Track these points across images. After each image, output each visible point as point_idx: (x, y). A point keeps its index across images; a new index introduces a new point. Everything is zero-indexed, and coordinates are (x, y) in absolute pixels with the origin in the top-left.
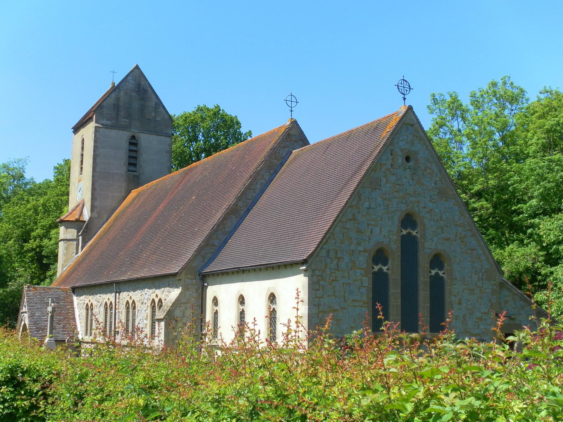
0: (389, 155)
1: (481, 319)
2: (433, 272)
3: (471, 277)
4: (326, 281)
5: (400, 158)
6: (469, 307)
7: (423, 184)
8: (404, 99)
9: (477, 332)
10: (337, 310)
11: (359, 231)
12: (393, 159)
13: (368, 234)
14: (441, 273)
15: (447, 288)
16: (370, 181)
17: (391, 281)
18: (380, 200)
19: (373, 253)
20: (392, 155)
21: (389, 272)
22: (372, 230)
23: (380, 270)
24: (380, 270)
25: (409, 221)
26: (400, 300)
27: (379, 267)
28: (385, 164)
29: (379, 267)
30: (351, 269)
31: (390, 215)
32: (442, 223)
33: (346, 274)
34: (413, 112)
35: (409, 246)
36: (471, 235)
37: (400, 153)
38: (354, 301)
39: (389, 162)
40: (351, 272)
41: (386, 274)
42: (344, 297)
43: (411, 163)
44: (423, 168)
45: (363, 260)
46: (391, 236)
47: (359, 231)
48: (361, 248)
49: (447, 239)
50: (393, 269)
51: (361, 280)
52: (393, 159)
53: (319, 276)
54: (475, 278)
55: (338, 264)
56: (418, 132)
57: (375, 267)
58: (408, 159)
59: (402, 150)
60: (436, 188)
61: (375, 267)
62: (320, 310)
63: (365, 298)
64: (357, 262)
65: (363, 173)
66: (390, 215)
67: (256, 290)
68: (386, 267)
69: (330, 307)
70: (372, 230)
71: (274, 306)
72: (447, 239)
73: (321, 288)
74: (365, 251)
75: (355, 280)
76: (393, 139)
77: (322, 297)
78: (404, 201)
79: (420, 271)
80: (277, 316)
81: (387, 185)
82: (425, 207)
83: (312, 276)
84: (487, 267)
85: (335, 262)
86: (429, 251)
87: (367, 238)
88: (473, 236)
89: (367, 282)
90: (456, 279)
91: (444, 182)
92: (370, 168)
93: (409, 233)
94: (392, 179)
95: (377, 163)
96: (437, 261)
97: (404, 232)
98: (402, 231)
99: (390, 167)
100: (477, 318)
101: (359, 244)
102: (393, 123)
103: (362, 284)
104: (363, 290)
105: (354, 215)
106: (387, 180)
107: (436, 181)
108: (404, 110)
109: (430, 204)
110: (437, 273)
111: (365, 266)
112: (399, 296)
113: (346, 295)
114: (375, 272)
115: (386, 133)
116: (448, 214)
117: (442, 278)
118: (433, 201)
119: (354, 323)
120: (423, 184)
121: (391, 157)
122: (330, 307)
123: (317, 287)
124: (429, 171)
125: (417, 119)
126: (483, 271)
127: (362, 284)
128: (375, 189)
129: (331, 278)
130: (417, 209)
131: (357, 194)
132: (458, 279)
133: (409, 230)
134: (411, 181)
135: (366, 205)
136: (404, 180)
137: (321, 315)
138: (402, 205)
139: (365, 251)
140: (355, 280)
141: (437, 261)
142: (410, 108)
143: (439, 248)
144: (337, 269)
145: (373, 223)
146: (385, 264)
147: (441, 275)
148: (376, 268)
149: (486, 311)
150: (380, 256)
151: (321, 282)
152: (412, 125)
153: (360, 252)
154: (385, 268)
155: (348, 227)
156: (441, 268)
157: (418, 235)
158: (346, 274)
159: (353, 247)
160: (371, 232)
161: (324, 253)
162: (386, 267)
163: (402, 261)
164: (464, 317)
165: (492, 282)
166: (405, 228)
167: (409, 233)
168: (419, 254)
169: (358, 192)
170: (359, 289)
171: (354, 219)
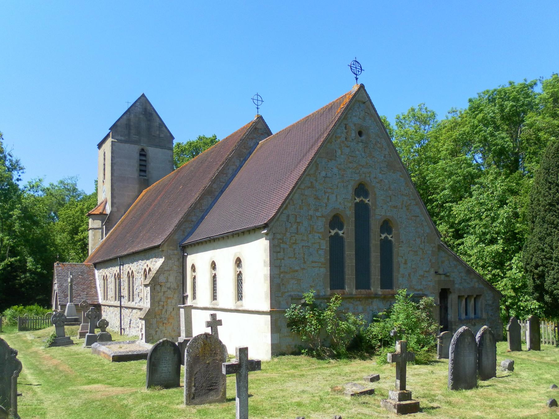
0: (344, 128)
1: (423, 276)
2: (383, 236)
3: (415, 240)
4: (286, 243)
5: (353, 132)
6: (413, 266)
7: (374, 157)
8: (357, 79)
9: (419, 287)
10: (297, 271)
11: (317, 198)
12: (347, 133)
13: (326, 201)
14: (389, 237)
15: (395, 250)
16: (326, 152)
17: (346, 244)
18: (335, 170)
19: (330, 218)
20: (346, 128)
21: (344, 236)
22: (328, 197)
23: (337, 234)
24: (337, 234)
25: (361, 190)
26: (354, 261)
27: (335, 231)
28: (340, 137)
29: (335, 231)
30: (310, 233)
31: (345, 184)
32: (390, 192)
33: (305, 238)
34: (365, 90)
35: (362, 213)
36: (415, 203)
37: (354, 128)
38: (313, 262)
39: (344, 136)
40: (310, 236)
41: (342, 238)
42: (304, 258)
43: (363, 138)
44: (374, 143)
45: (321, 225)
46: (346, 203)
47: (317, 198)
48: (318, 214)
49: (395, 207)
50: (348, 233)
51: (319, 243)
52: (347, 133)
53: (280, 239)
54: (418, 241)
55: (297, 228)
56: (369, 109)
57: (331, 231)
58: (360, 134)
59: (355, 125)
60: (385, 161)
61: (331, 231)
62: (282, 270)
63: (323, 260)
64: (315, 227)
65: (319, 144)
66: (345, 184)
67: (224, 256)
68: (342, 232)
69: (291, 268)
70: (328, 197)
71: (240, 270)
72: (395, 207)
73: (282, 251)
74: (322, 216)
75: (314, 243)
76: (346, 114)
77: (283, 259)
78: (357, 171)
79: (372, 235)
80: (243, 278)
81: (342, 156)
82: (375, 178)
83: (273, 239)
84: (427, 231)
85: (295, 227)
86: (379, 217)
87: (325, 205)
88: (416, 205)
89: (325, 245)
90: (402, 242)
91: (392, 156)
92: (326, 139)
93: (362, 201)
94: (347, 151)
95: (332, 136)
96: (386, 226)
97: (358, 200)
98: (355, 199)
99: (344, 140)
100: (420, 276)
101: (317, 210)
102: (347, 100)
103: (320, 246)
105: (312, 182)
106: (342, 152)
107: (385, 155)
108: (356, 88)
109: (380, 175)
110: (386, 237)
111: (323, 230)
112: (354, 257)
113: (306, 257)
114: (331, 236)
115: (339, 111)
116: (395, 185)
117: (390, 241)
118: (383, 172)
119: (313, 282)
120: (374, 157)
121: (345, 131)
122: (291, 268)
123: (278, 250)
124: (379, 145)
125: (369, 97)
126: (425, 235)
127: (320, 246)
128: (331, 160)
129: (292, 241)
130: (369, 179)
131: (314, 163)
132: (404, 242)
133: (362, 198)
134: (363, 154)
135: (323, 174)
136: (357, 152)
137: (282, 275)
138: (356, 175)
139: (322, 216)
140: (314, 243)
141: (386, 226)
142: (362, 86)
143: (388, 214)
144: (297, 233)
145: (329, 191)
146: (341, 229)
147: (390, 238)
148: (333, 233)
149: (428, 269)
150: (336, 221)
151: (282, 245)
152: (364, 103)
153: (318, 217)
154: (340, 233)
155: (306, 193)
156: (390, 232)
157: (370, 203)
158: (305, 238)
159: (311, 213)
160: (328, 199)
161: (284, 218)
162: (342, 232)
163: (356, 227)
164: (409, 275)
165: (433, 245)
166: (359, 197)
167: (362, 201)
168: (371, 220)
169: (316, 162)
170: (317, 251)
171: (312, 187)
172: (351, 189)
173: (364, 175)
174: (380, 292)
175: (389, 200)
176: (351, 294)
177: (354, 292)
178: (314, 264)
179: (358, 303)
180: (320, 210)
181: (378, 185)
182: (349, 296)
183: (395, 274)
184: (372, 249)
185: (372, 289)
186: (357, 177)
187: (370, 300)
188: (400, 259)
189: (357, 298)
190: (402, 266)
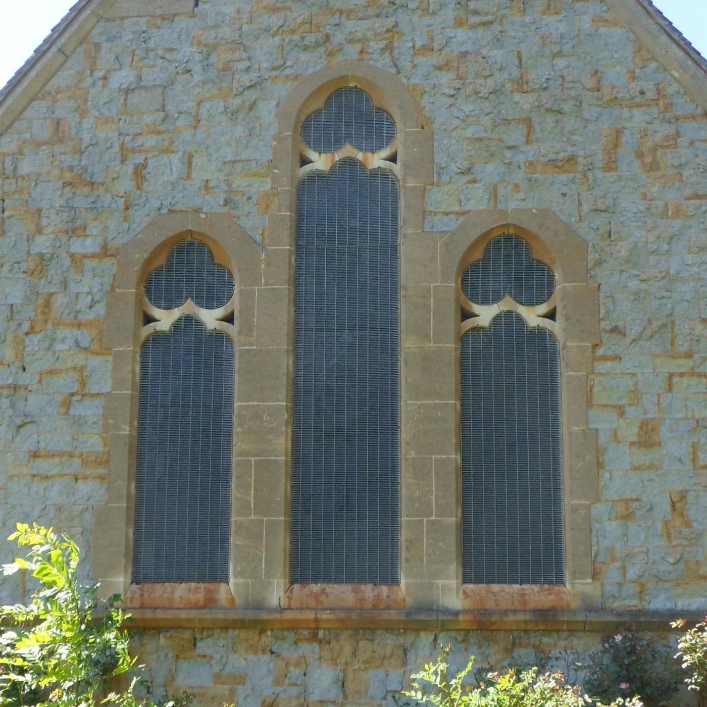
13: (126, 184)
27: (177, 313)
30: (32, 331)
38: (35, 455)
40: (33, 343)
46: (239, 183)
51: (80, 369)
57: (156, 312)
63: (93, 443)
68: (219, 312)
86: (452, 224)
89: (112, 376)
101: (75, 230)
103: (83, 383)
104: (90, 410)
127: (83, 383)
132: (632, 334)
138: (304, 57)
146: (210, 301)
153: (77, 261)
154: (210, 318)
157: (397, 168)
162: (219, 312)
166: (326, 145)
172: (271, 115)
173: (353, 51)
174: (453, 593)
175: (516, 135)
176: (259, 606)
177: (276, 593)
178: (43, 465)
179: (309, 649)
180: (94, 228)
181: (446, 79)
182: (250, 615)
183: (570, 500)
184: (407, 377)
185: (403, 581)
186: (312, 65)
187: (388, 642)
188: (603, 422)
189: (294, 627)
190: (621, 460)
